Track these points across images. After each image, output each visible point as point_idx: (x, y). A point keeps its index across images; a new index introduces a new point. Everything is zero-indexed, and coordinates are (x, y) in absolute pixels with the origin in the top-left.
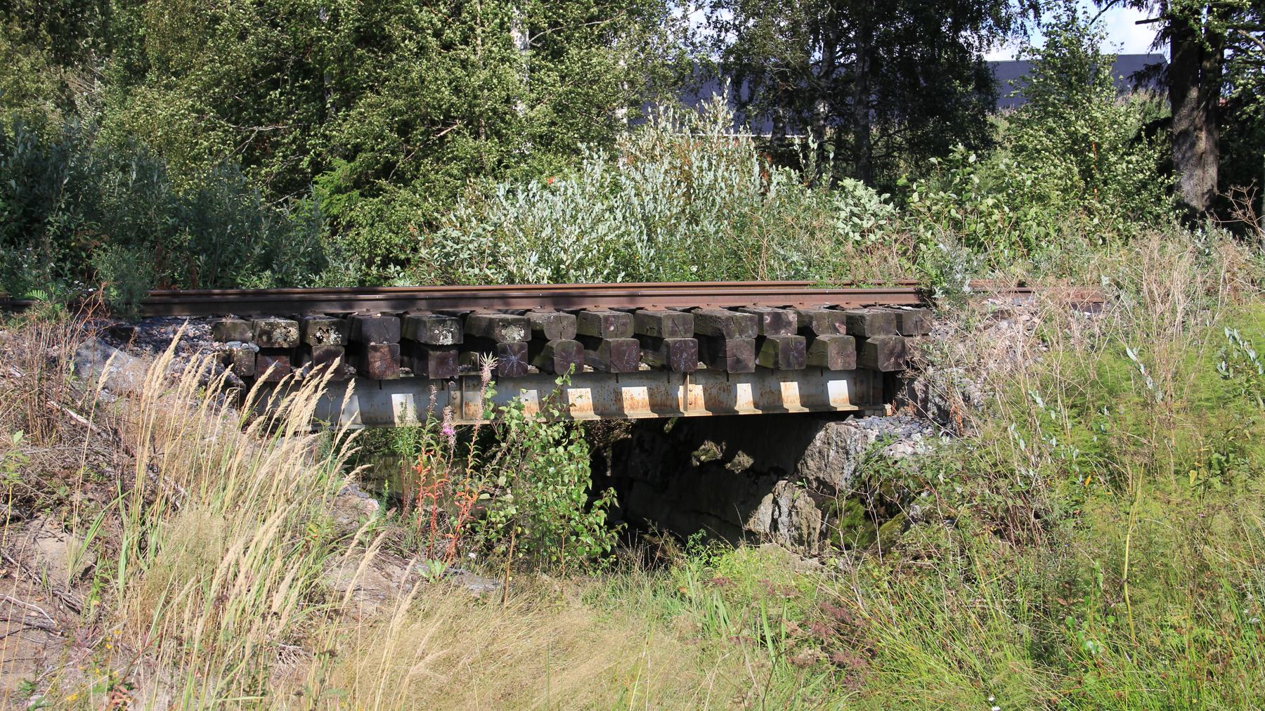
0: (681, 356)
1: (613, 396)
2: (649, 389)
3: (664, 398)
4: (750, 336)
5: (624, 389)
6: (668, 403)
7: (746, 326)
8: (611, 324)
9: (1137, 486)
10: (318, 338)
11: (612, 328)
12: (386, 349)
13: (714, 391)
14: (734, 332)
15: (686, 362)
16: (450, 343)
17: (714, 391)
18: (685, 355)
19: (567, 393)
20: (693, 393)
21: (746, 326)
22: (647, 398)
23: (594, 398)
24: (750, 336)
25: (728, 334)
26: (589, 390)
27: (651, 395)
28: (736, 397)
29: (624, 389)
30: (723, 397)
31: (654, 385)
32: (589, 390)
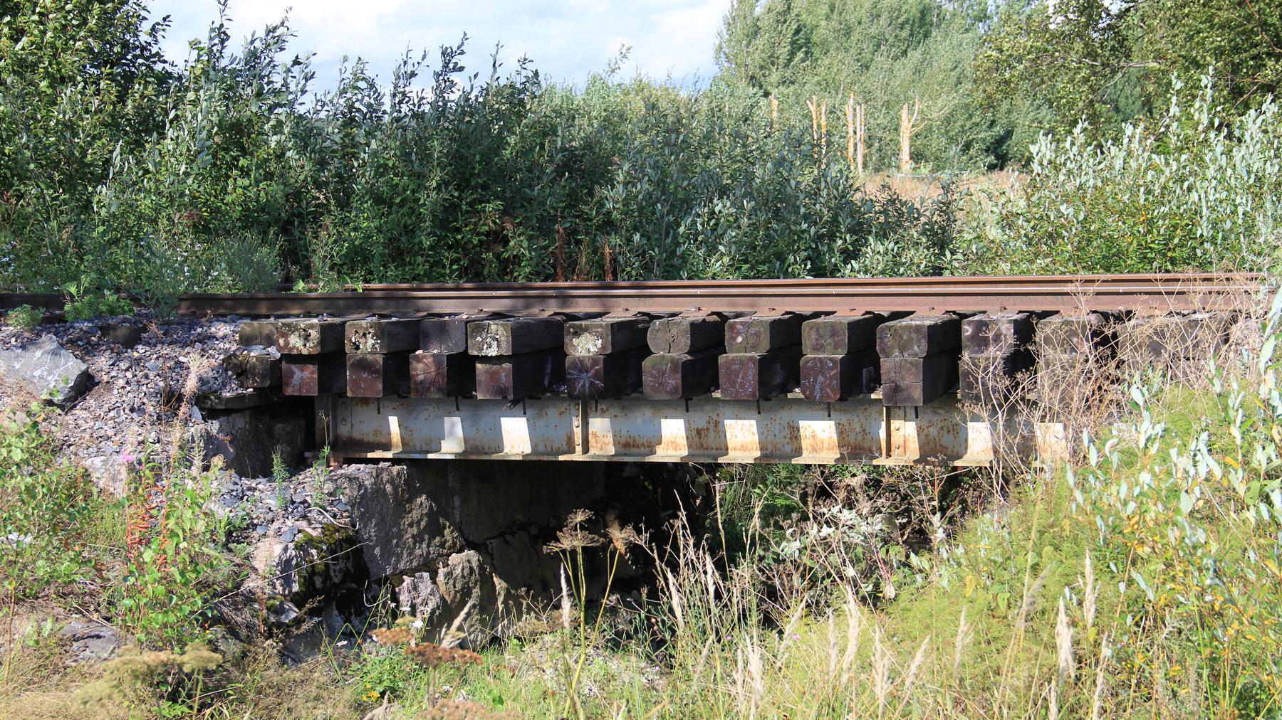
0: (815, 381)
1: (787, 432)
2: (838, 425)
3: (860, 437)
4: (916, 355)
5: (802, 423)
6: (866, 445)
7: (910, 339)
8: (739, 334)
9: (627, 681)
10: (354, 344)
11: (740, 339)
12: (431, 360)
13: (933, 431)
14: (893, 348)
15: (822, 389)
16: (494, 354)
17: (933, 431)
18: (821, 378)
19: (723, 426)
20: (901, 432)
21: (910, 339)
22: (835, 437)
23: (760, 434)
24: (916, 355)
25: (883, 350)
26: (753, 422)
27: (841, 433)
28: (966, 440)
29: (802, 423)
30: (947, 439)
31: (844, 419)
32: (753, 422)
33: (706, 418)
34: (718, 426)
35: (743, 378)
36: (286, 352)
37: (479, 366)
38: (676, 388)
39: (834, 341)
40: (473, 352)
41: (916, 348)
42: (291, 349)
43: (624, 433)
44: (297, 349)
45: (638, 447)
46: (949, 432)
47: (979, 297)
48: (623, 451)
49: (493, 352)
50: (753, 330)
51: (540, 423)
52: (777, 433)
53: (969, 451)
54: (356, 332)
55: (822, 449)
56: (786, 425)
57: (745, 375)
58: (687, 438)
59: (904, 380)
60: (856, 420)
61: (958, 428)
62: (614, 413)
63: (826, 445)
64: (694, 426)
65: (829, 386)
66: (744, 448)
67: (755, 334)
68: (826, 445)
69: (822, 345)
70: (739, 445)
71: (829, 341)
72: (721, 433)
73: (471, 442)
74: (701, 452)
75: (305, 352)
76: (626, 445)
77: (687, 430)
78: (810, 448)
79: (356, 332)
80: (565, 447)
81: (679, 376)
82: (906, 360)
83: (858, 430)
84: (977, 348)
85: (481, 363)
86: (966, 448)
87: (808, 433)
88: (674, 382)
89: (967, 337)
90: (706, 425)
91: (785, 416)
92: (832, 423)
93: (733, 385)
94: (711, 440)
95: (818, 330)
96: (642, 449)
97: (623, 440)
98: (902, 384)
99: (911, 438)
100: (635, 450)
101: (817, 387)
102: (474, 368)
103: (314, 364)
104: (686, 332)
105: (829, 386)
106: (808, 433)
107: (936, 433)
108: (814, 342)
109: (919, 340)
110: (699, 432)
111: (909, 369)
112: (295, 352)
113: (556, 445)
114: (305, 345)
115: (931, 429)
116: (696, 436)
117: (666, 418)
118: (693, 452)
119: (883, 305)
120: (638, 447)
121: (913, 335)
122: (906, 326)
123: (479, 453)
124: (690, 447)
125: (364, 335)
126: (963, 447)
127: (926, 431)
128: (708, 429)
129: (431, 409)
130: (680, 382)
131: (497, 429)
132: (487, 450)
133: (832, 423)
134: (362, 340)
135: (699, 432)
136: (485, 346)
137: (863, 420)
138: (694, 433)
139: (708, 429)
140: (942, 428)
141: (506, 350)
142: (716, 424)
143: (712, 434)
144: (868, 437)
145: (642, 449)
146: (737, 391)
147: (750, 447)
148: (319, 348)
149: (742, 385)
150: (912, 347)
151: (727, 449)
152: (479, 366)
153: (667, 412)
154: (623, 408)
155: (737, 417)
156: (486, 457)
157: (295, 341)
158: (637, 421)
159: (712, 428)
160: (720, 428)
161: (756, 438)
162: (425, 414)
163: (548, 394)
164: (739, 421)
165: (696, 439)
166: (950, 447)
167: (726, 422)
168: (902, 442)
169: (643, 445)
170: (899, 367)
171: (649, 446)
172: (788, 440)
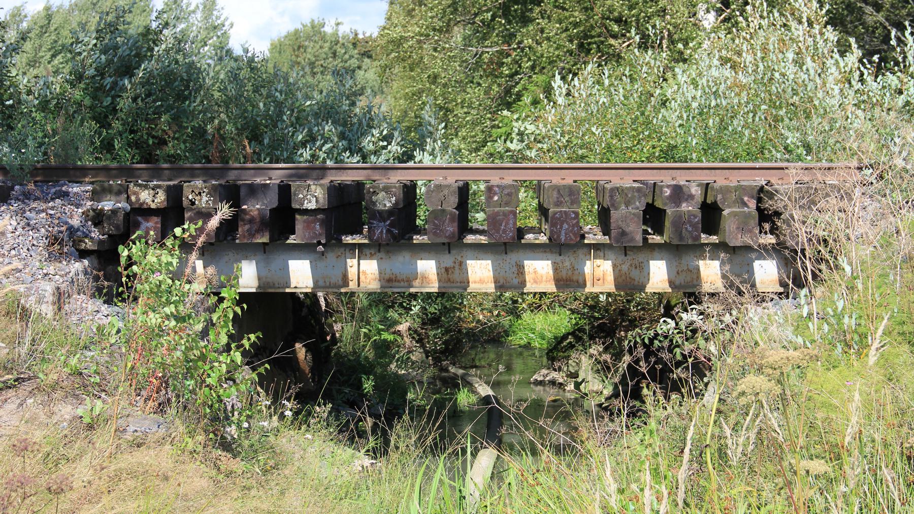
0: (561, 227)
1: (515, 269)
2: (554, 263)
3: (570, 273)
4: (637, 208)
5: (526, 263)
6: (575, 278)
7: (633, 197)
8: (495, 194)
10: (191, 201)
11: (496, 198)
13: (625, 268)
14: (620, 203)
15: (566, 234)
16: (314, 207)
17: (625, 268)
18: (565, 226)
19: (466, 265)
20: (601, 268)
21: (633, 197)
22: (551, 272)
23: (494, 271)
24: (637, 208)
25: (613, 205)
26: (489, 262)
27: (556, 270)
28: (649, 274)
29: (526, 263)
30: (635, 274)
31: (559, 259)
32: (489, 262)
33: (452, 259)
34: (462, 265)
35: (505, 226)
36: (137, 206)
37: (298, 217)
38: (453, 233)
39: (571, 199)
40: (295, 206)
41: (637, 203)
42: (142, 204)
43: (388, 271)
44: (147, 204)
45: (399, 281)
46: (636, 268)
47: (655, 171)
48: (387, 284)
49: (312, 205)
50: (506, 191)
51: (321, 264)
52: (508, 270)
53: (651, 281)
54: (193, 191)
55: (541, 282)
56: (514, 264)
57: (507, 224)
58: (438, 274)
59: (629, 226)
60: (567, 259)
61: (643, 265)
62: (380, 257)
63: (544, 278)
64: (444, 265)
65: (571, 231)
66: (481, 281)
67: (508, 194)
68: (544, 278)
69: (562, 202)
70: (478, 279)
71: (567, 199)
72: (464, 270)
73: (264, 280)
74: (449, 284)
75: (153, 206)
76: (389, 280)
77: (438, 268)
78: (532, 281)
79: (193, 191)
80: (340, 282)
81: (456, 224)
82: (630, 212)
83: (568, 267)
84: (673, 205)
85: (300, 214)
86: (649, 280)
87: (531, 270)
88: (451, 229)
89: (666, 196)
90: (452, 265)
91: (513, 257)
92: (550, 262)
93: (498, 231)
94: (456, 276)
95: (559, 191)
96: (402, 283)
97: (387, 277)
98: (627, 230)
99: (608, 272)
100: (397, 284)
101: (563, 232)
102: (294, 219)
103: (158, 216)
104: (455, 192)
105: (571, 231)
106: (531, 270)
107: (627, 269)
108: (556, 200)
109: (640, 197)
110: (447, 270)
111: (632, 219)
112: (145, 206)
113: (333, 281)
114: (153, 201)
115: (623, 266)
116: (445, 273)
117: (421, 259)
118: (442, 285)
119: (584, 176)
120: (399, 281)
121: (636, 194)
122: (630, 187)
123: (271, 287)
124: (440, 281)
125: (200, 193)
126: (647, 278)
127: (619, 267)
128: (454, 267)
129: (231, 254)
130: (456, 230)
131: (286, 269)
132: (277, 285)
133: (550, 262)
134: (198, 198)
135: (447, 270)
136: (306, 202)
137: (572, 259)
138: (443, 270)
139: (454, 267)
140: (631, 265)
141: (323, 202)
142: (461, 264)
143: (457, 271)
144: (576, 272)
145: (402, 283)
146: (501, 236)
147: (486, 281)
148: (165, 203)
149: (504, 231)
150: (635, 203)
151: (469, 282)
152: (298, 217)
153: (423, 255)
154: (388, 252)
155: (477, 259)
156: (281, 291)
157: (145, 196)
158: (399, 262)
159: (457, 267)
160: (463, 266)
161: (491, 274)
162: (226, 258)
163: (334, 241)
164: (478, 261)
165: (445, 275)
166: (637, 279)
167: (468, 262)
168: (602, 275)
169: (403, 280)
170: (625, 218)
171: (407, 281)
172: (515, 275)
